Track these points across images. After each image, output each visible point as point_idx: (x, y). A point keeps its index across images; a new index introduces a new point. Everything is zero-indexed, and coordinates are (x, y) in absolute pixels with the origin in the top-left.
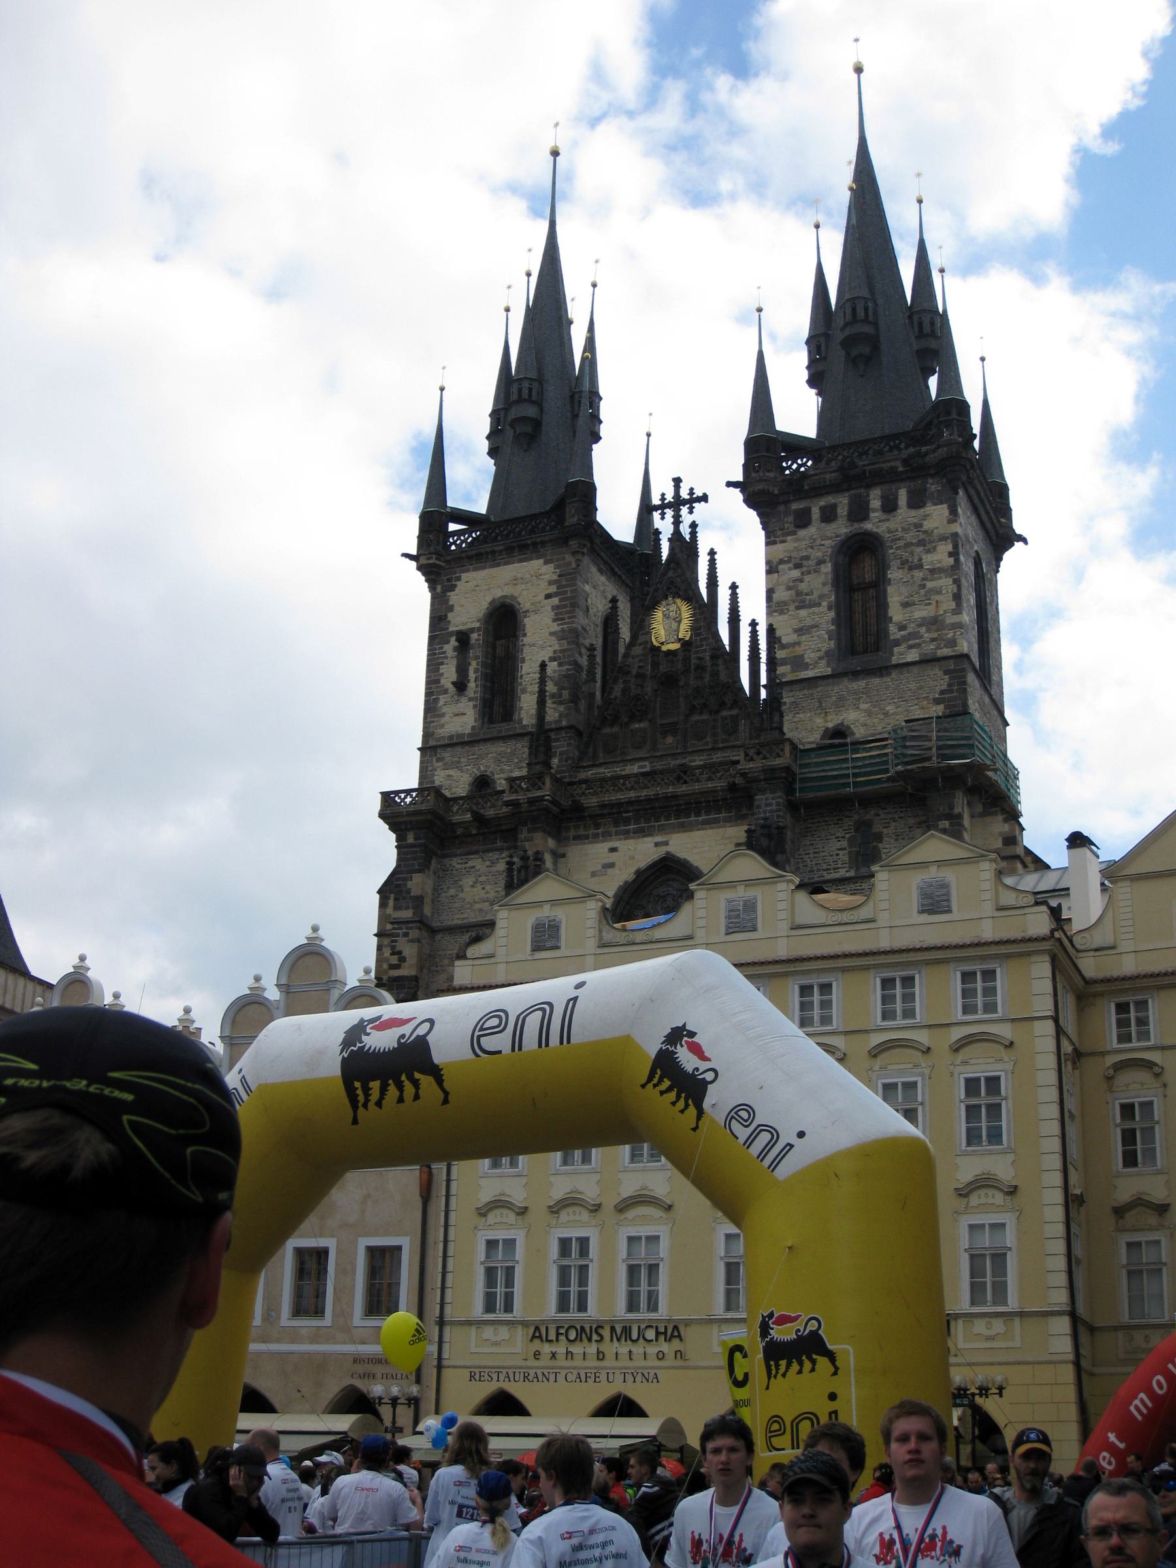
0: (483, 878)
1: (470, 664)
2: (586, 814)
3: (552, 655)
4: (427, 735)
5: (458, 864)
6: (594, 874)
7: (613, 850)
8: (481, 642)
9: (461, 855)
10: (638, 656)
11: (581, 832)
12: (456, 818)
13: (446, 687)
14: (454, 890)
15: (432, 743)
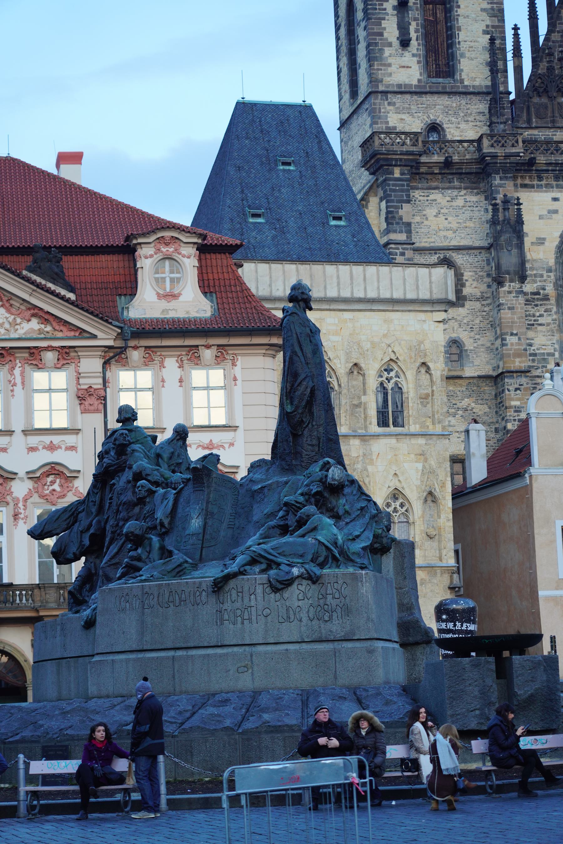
0: (446, 211)
1: (410, 24)
2: (534, 168)
3: (485, 28)
4: (373, 80)
5: (420, 196)
6: (541, 217)
7: (555, 199)
8: (419, 6)
9: (422, 189)
10: (557, 42)
11: (527, 182)
12: (424, 159)
13: (390, 40)
14: (419, 218)
15: (381, 88)
